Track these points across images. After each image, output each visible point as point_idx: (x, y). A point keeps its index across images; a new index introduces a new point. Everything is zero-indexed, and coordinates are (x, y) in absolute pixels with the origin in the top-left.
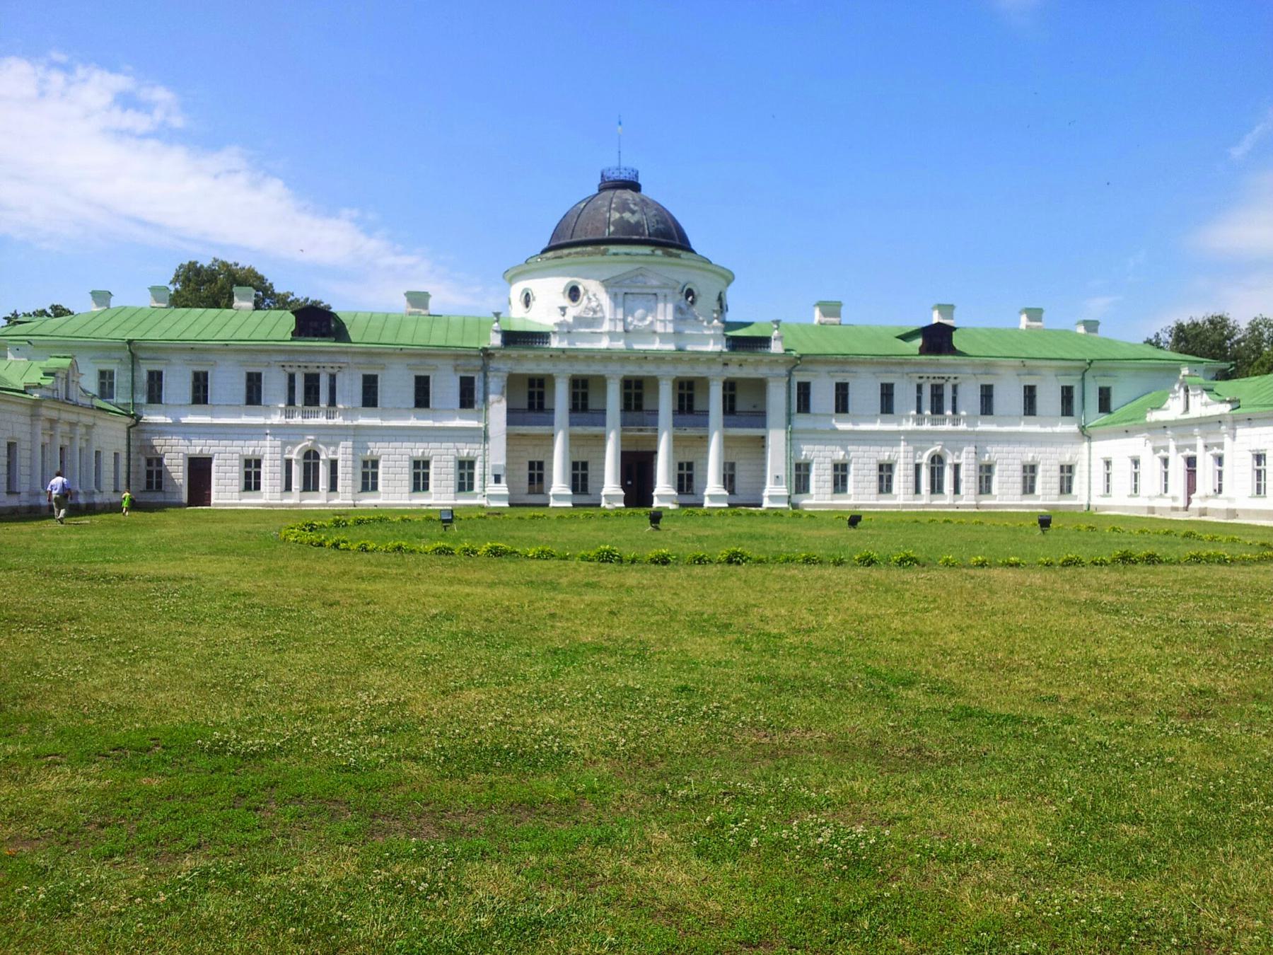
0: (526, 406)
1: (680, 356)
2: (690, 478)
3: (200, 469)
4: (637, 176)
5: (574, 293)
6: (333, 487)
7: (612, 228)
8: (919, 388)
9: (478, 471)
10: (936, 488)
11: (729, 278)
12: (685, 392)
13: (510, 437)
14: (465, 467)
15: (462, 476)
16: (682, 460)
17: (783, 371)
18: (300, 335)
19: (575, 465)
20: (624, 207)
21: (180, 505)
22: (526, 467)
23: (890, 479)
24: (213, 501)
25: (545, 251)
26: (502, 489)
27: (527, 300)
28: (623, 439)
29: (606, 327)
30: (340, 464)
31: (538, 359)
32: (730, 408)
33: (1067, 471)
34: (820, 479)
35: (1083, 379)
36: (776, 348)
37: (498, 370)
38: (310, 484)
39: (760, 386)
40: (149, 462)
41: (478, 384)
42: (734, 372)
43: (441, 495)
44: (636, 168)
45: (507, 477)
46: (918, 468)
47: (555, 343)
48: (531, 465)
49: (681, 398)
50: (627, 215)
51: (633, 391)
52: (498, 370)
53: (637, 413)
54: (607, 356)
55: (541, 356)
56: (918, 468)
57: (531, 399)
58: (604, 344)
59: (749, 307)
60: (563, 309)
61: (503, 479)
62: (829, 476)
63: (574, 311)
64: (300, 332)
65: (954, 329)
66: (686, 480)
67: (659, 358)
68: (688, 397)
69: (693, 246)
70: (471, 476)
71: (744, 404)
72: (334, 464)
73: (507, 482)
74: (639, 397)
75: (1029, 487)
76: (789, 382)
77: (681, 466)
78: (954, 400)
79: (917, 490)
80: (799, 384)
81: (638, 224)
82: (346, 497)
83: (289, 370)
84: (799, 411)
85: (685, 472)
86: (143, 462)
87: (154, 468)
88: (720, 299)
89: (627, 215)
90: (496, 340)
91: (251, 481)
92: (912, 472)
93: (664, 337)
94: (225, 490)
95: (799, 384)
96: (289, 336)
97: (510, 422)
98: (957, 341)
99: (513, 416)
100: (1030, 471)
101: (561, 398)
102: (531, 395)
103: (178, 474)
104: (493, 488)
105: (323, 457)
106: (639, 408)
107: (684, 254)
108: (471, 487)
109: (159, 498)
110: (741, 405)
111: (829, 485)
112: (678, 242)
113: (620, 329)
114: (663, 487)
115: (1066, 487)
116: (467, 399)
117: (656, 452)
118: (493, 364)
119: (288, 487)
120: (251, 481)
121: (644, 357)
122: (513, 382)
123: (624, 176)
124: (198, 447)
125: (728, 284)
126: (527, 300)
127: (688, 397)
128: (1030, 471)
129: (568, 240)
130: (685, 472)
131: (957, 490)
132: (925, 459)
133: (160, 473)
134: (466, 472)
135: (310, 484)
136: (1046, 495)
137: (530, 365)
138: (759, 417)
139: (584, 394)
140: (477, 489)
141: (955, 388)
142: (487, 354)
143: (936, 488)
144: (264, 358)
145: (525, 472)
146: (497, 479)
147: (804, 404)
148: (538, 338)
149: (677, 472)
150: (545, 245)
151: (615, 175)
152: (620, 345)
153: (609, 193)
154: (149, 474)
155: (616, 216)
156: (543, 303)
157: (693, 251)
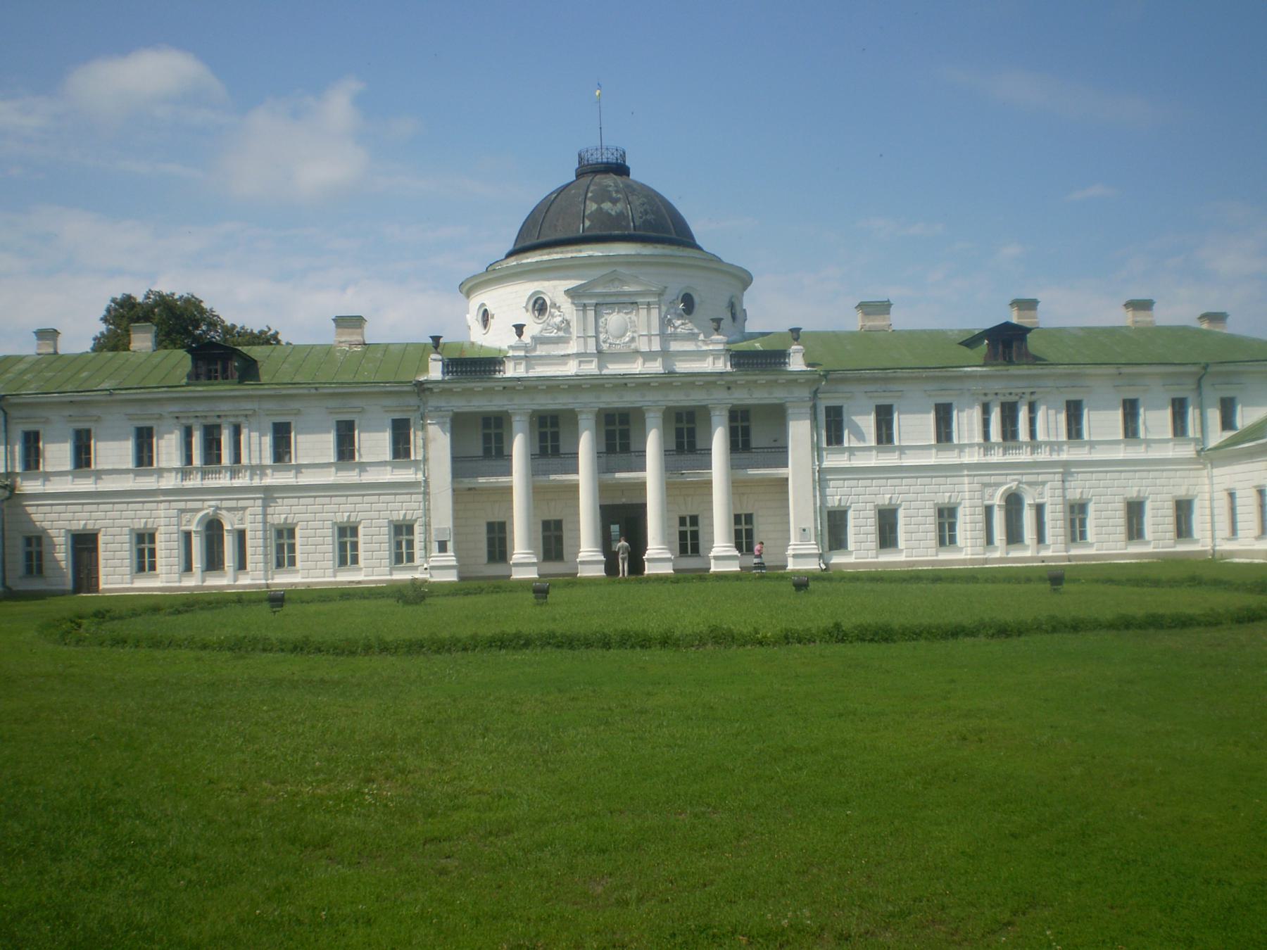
0: (480, 453)
1: (669, 380)
2: (695, 535)
3: (85, 545)
4: (623, 155)
5: (540, 306)
6: (242, 565)
7: (587, 223)
8: (986, 410)
9: (418, 537)
10: (1014, 536)
11: (744, 279)
12: (685, 425)
13: (456, 493)
14: (402, 530)
15: (399, 545)
16: (684, 513)
17: (805, 393)
18: (197, 377)
19: (546, 525)
20: (604, 195)
21: (63, 593)
22: (484, 530)
23: (952, 527)
24: (102, 586)
25: (510, 255)
26: (450, 558)
27: (486, 317)
28: (603, 489)
29: (573, 348)
30: (248, 535)
31: (488, 392)
32: (739, 443)
33: (1183, 509)
34: (861, 531)
35: (1199, 387)
36: (796, 363)
37: (438, 409)
38: (214, 563)
39: (778, 415)
40: (29, 541)
42: (742, 397)
43: (373, 568)
45: (455, 543)
46: (989, 510)
48: (491, 526)
49: (679, 433)
50: (607, 206)
51: (617, 427)
52: (438, 409)
53: (624, 456)
54: (575, 385)
55: (492, 389)
56: (989, 510)
57: (481, 442)
58: (571, 368)
59: (766, 314)
60: (519, 329)
61: (450, 545)
62: (871, 526)
63: (533, 328)
64: (194, 377)
65: (1028, 330)
66: (689, 539)
67: (643, 383)
69: (698, 242)
70: (410, 544)
71: (755, 436)
72: (241, 535)
73: (455, 551)
74: (625, 435)
75: (1135, 530)
76: (814, 408)
77: (682, 521)
78: (1032, 422)
79: (989, 540)
80: (827, 408)
81: (621, 215)
82: (255, 577)
83: (184, 421)
84: (829, 443)
85: (688, 528)
86: (20, 543)
87: (34, 549)
89: (607, 206)
90: (435, 371)
91: (144, 560)
92: (981, 518)
93: (649, 356)
94: (115, 575)
95: (827, 408)
96: (185, 381)
97: (457, 473)
98: (1034, 343)
99: (461, 464)
100: (1135, 511)
102: (487, 438)
103: (62, 555)
104: (437, 558)
105: (227, 527)
108: (411, 558)
109: (36, 585)
110: (758, 438)
111: (873, 539)
112: (674, 236)
113: (592, 348)
114: (658, 553)
115: (1183, 529)
116: (401, 449)
117: (645, 505)
118: (433, 402)
119: (188, 568)
120: (144, 560)
121: (623, 383)
122: (459, 425)
123: (609, 157)
124: (82, 519)
125: (745, 288)
126: (486, 317)
128: (1135, 511)
129: (535, 241)
130: (688, 528)
131: (1040, 538)
132: (997, 500)
133: (40, 554)
135: (214, 563)
136: (1158, 538)
138: (779, 454)
140: (417, 561)
141: (1032, 409)
142: (422, 389)
143: (1014, 536)
144: (155, 410)
146: (443, 547)
149: (676, 529)
150: (510, 246)
151: (597, 157)
152: (591, 368)
153: (586, 180)
154: (29, 556)
155: (592, 207)
156: (509, 319)
157: (699, 248)
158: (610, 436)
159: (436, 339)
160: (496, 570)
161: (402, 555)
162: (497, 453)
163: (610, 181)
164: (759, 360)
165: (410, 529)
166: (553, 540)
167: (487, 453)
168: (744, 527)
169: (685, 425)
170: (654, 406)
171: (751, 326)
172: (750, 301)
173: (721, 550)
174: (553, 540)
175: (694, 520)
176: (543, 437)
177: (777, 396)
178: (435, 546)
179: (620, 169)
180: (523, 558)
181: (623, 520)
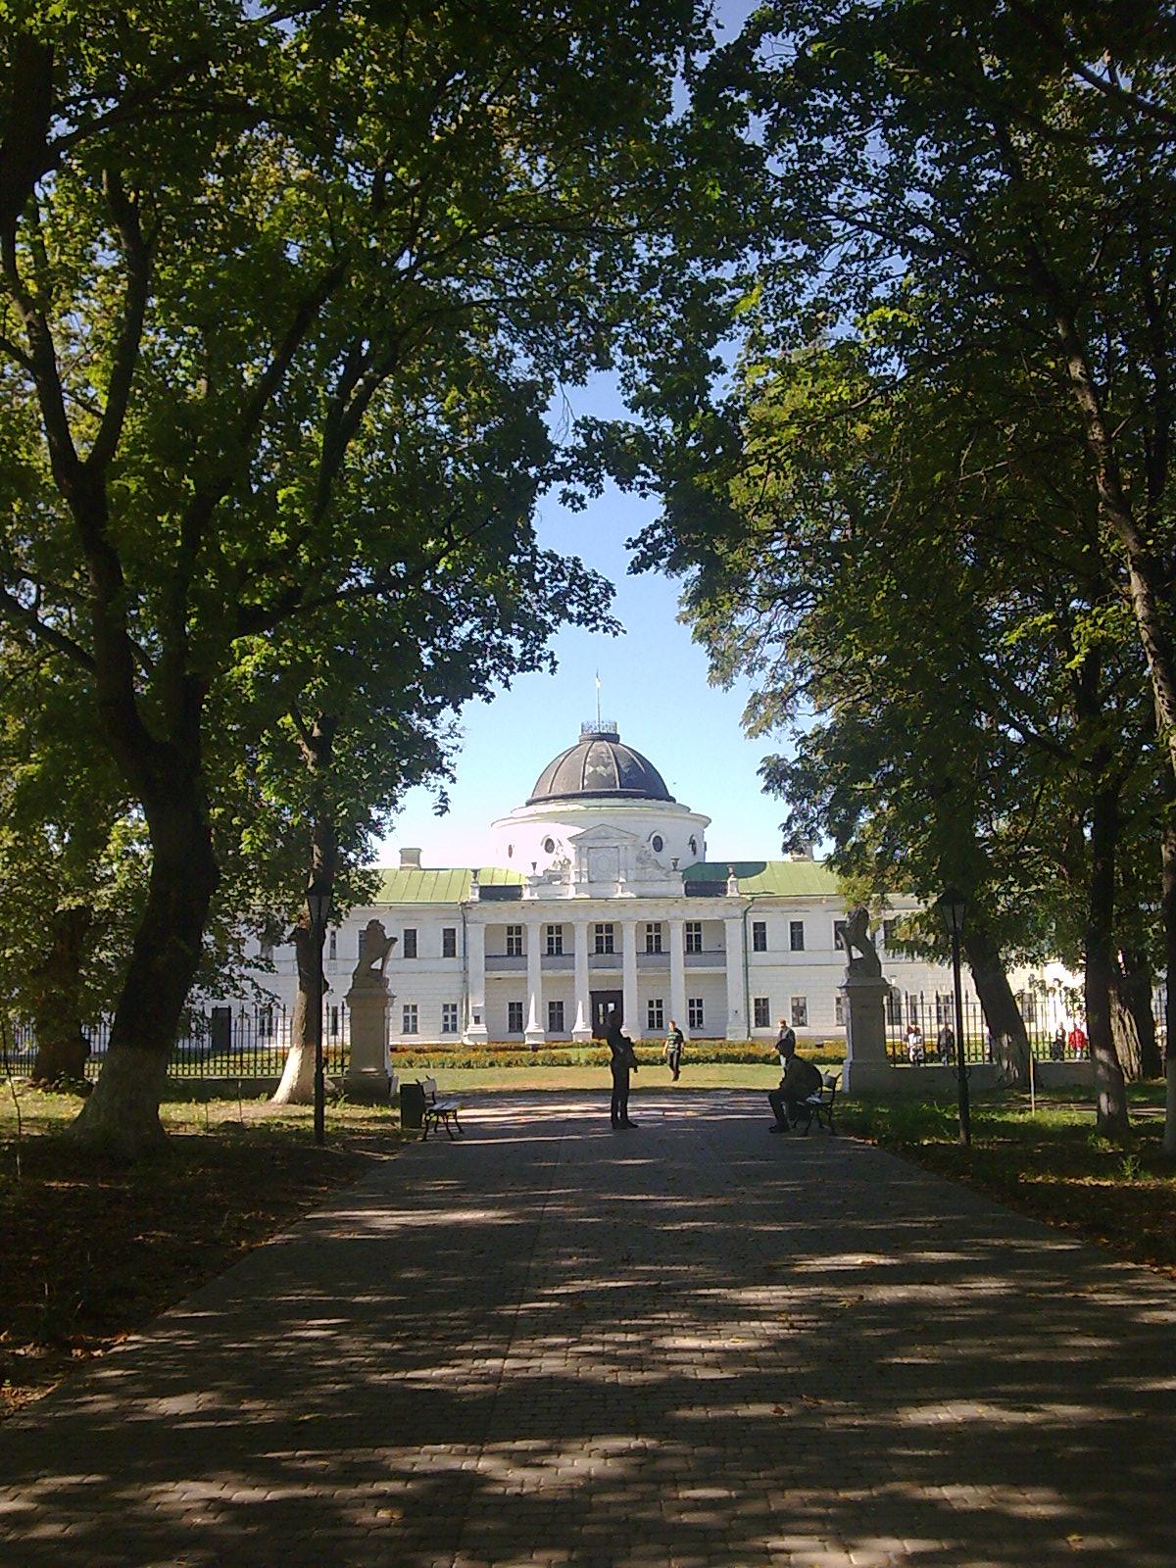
5: (549, 845)
11: (706, 821)
15: (446, 1018)
26: (482, 1029)
32: (693, 945)
39: (719, 925)
41: (459, 935)
44: (613, 719)
47: (526, 895)
50: (601, 769)
68: (654, 941)
74: (610, 940)
85: (655, 1009)
88: (693, 843)
101: (534, 944)
106: (610, 950)
130: (655, 1009)
134: (450, 1014)
146: (477, 1020)
147: (760, 944)
148: (511, 893)
149: (647, 1009)
150: (529, 797)
155: (590, 769)
158: (599, 940)
159: (475, 872)
160: (516, 1036)
161: (450, 1027)
163: (603, 747)
165: (454, 1008)
166: (556, 1017)
167: (510, 953)
168: (696, 1009)
169: (653, 934)
171: (711, 857)
172: (709, 835)
174: (556, 1017)
175: (659, 1003)
176: (550, 941)
178: (472, 1020)
179: (613, 738)
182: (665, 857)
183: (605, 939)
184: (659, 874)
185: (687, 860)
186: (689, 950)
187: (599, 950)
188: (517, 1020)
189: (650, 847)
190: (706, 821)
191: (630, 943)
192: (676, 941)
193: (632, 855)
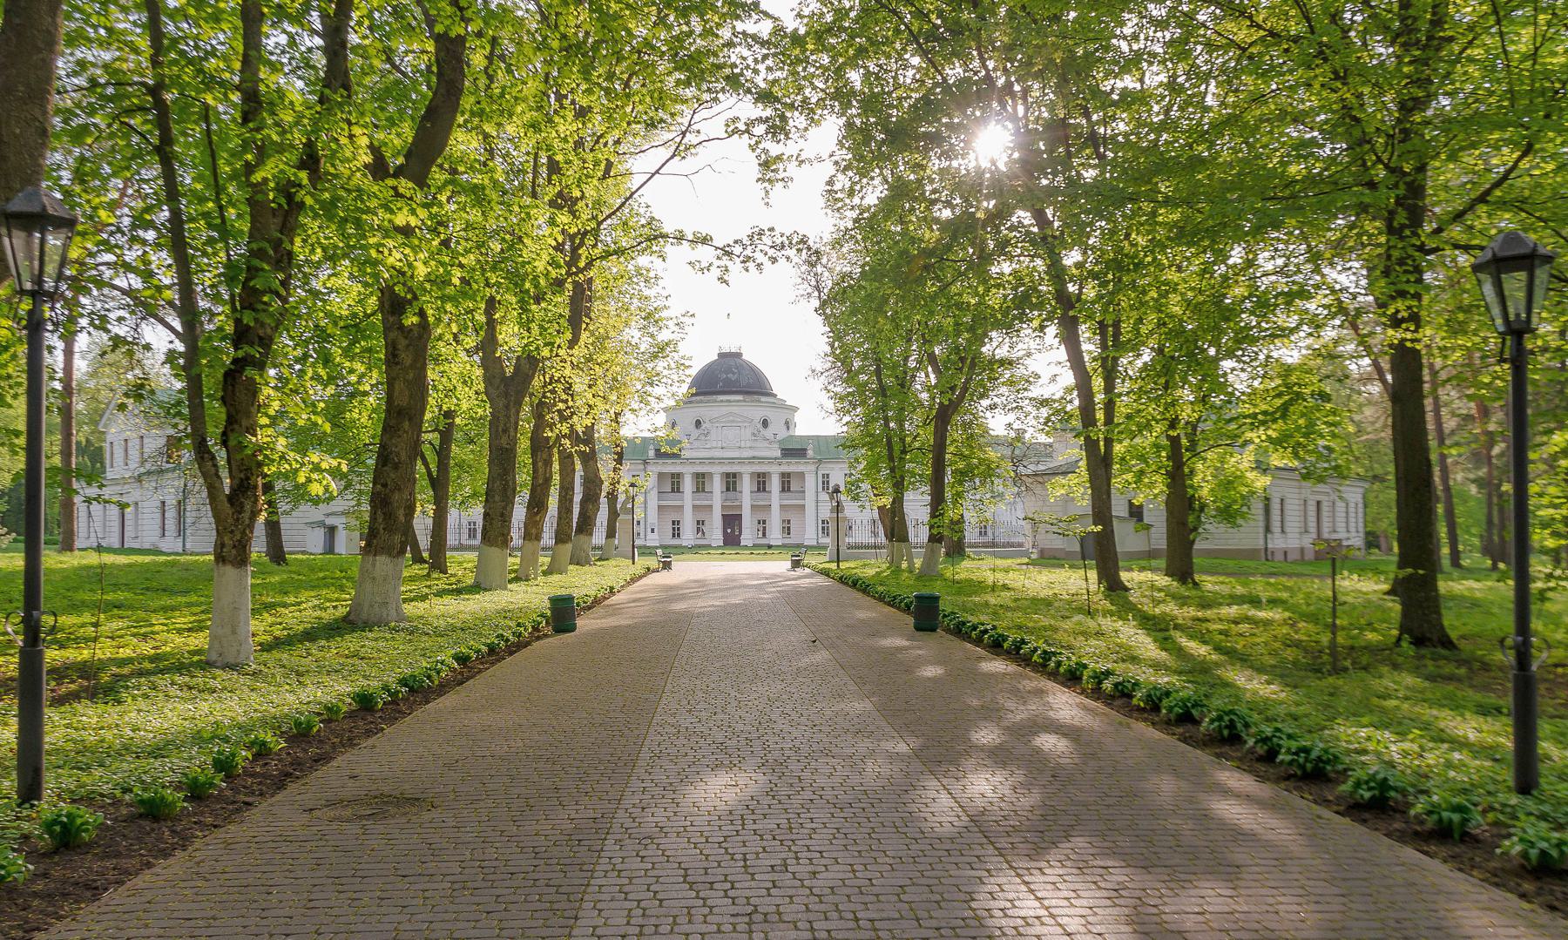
5: (698, 424)
11: (795, 409)
17: (813, 468)
36: (810, 453)
39: (802, 475)
42: (785, 469)
67: (741, 461)
68: (761, 482)
88: (787, 423)
101: (688, 485)
107: (763, 399)
114: (748, 536)
118: (649, 468)
121: (732, 460)
122: (661, 475)
127: (761, 482)
137: (670, 467)
139: (701, 480)
145: (670, 526)
162: (676, 489)
164: (794, 451)
170: (746, 471)
172: (798, 417)
173: (775, 536)
177: (801, 468)
179: (739, 355)
180: (688, 536)
181: (732, 521)
182: (768, 433)
183: (731, 481)
184: (766, 444)
185: (783, 434)
186: (783, 490)
187: (728, 489)
188: (676, 533)
189: (760, 426)
190: (795, 409)
191: (746, 485)
192: (775, 484)
193: (749, 432)
